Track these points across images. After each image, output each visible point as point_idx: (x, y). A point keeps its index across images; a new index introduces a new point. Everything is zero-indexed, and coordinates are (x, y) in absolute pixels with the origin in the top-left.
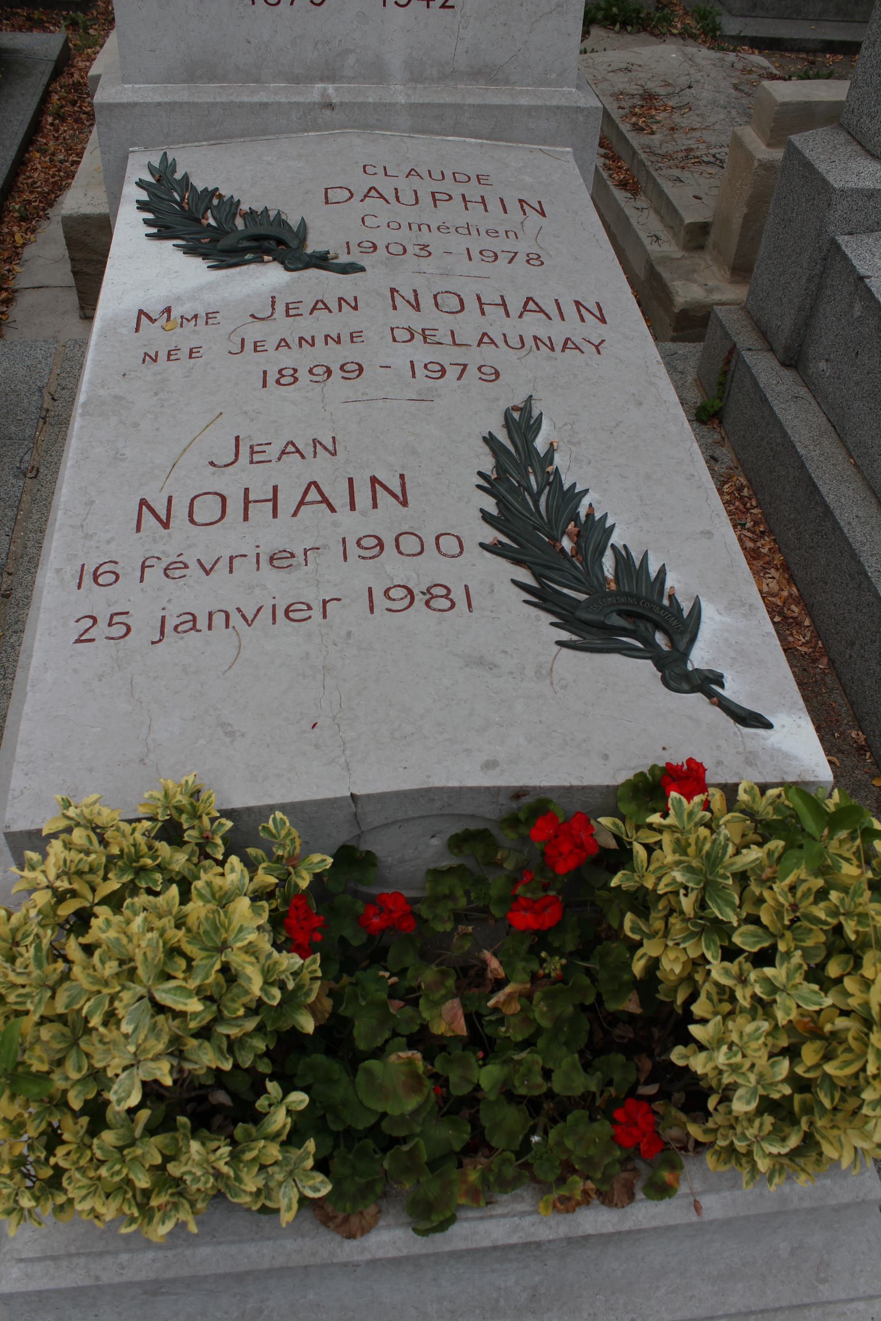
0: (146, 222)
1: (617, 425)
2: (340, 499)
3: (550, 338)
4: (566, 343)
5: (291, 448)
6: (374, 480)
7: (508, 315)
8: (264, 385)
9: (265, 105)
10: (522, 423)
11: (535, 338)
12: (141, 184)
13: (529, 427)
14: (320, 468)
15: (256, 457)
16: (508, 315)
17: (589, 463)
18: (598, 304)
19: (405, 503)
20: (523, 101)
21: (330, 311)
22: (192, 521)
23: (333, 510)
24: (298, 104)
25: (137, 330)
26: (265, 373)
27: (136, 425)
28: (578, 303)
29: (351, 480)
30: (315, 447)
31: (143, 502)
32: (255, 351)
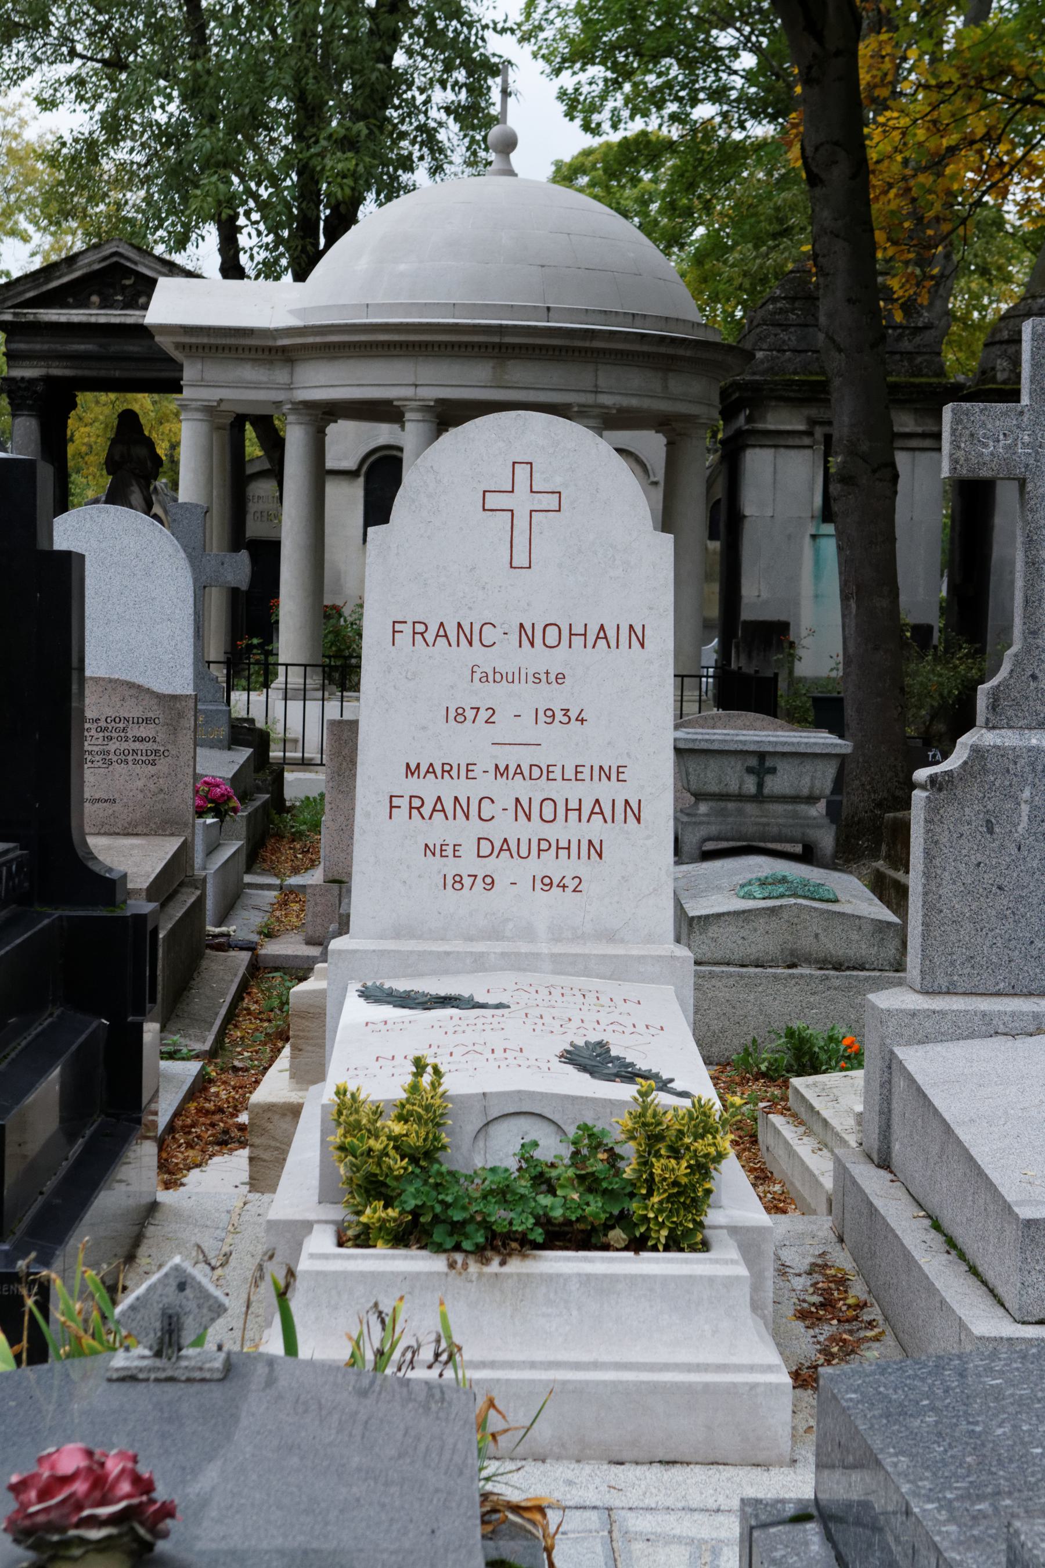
9: (447, 953)
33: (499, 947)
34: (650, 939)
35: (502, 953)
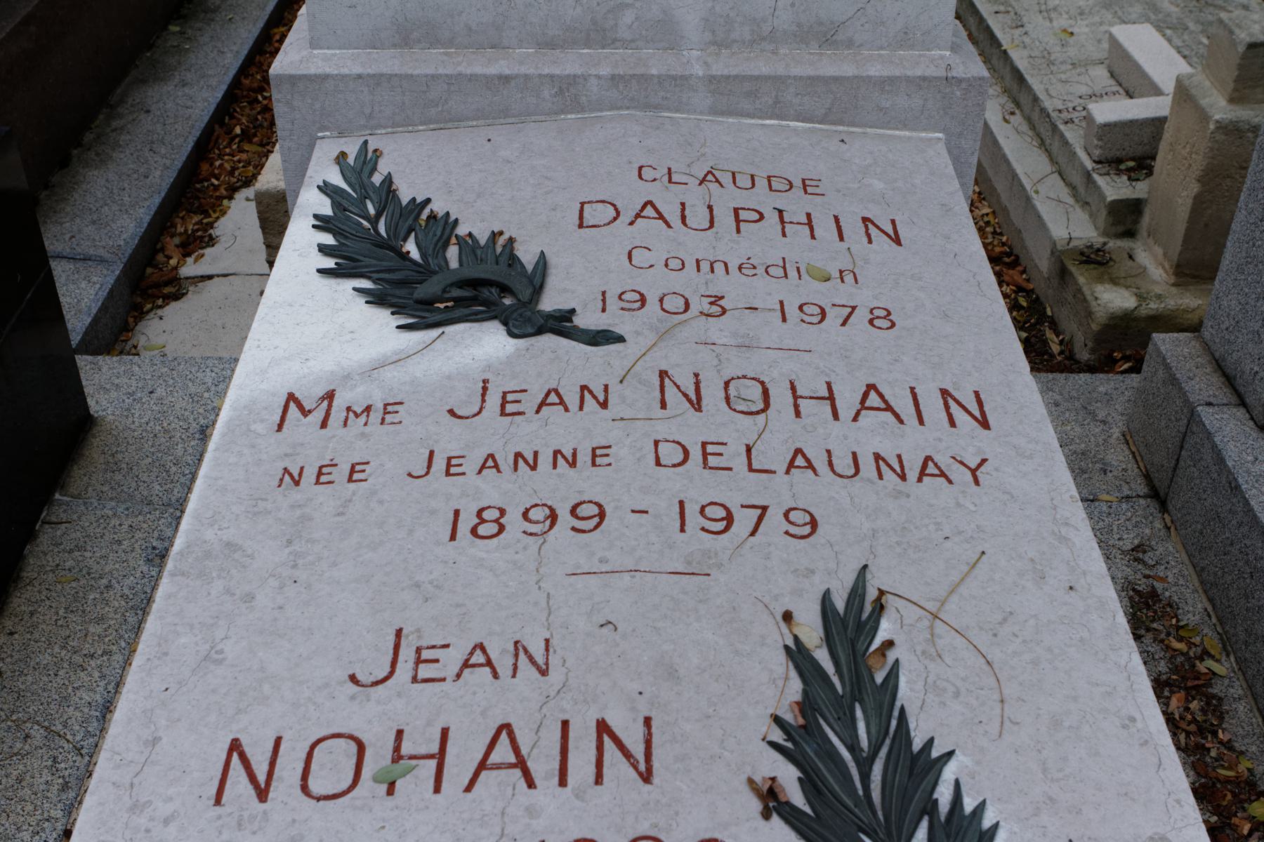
0: (323, 249)
1: (1005, 620)
2: (543, 764)
3: (899, 457)
4: (925, 466)
5: (478, 658)
6: (603, 727)
7: (836, 416)
8: (453, 538)
9: (505, 79)
10: (852, 623)
11: (877, 457)
12: (326, 188)
13: (860, 626)
14: (518, 699)
15: (425, 671)
16: (836, 416)
17: (957, 694)
18: (977, 394)
19: (647, 777)
20: (875, 70)
21: (567, 410)
22: (305, 788)
23: (531, 784)
24: (552, 76)
25: (280, 427)
26: (457, 513)
27: (249, 598)
28: (945, 393)
29: (565, 724)
30: (516, 656)
31: (235, 746)
32: (448, 474)
33: (606, 63)
34: (905, 40)
35: (613, 77)
